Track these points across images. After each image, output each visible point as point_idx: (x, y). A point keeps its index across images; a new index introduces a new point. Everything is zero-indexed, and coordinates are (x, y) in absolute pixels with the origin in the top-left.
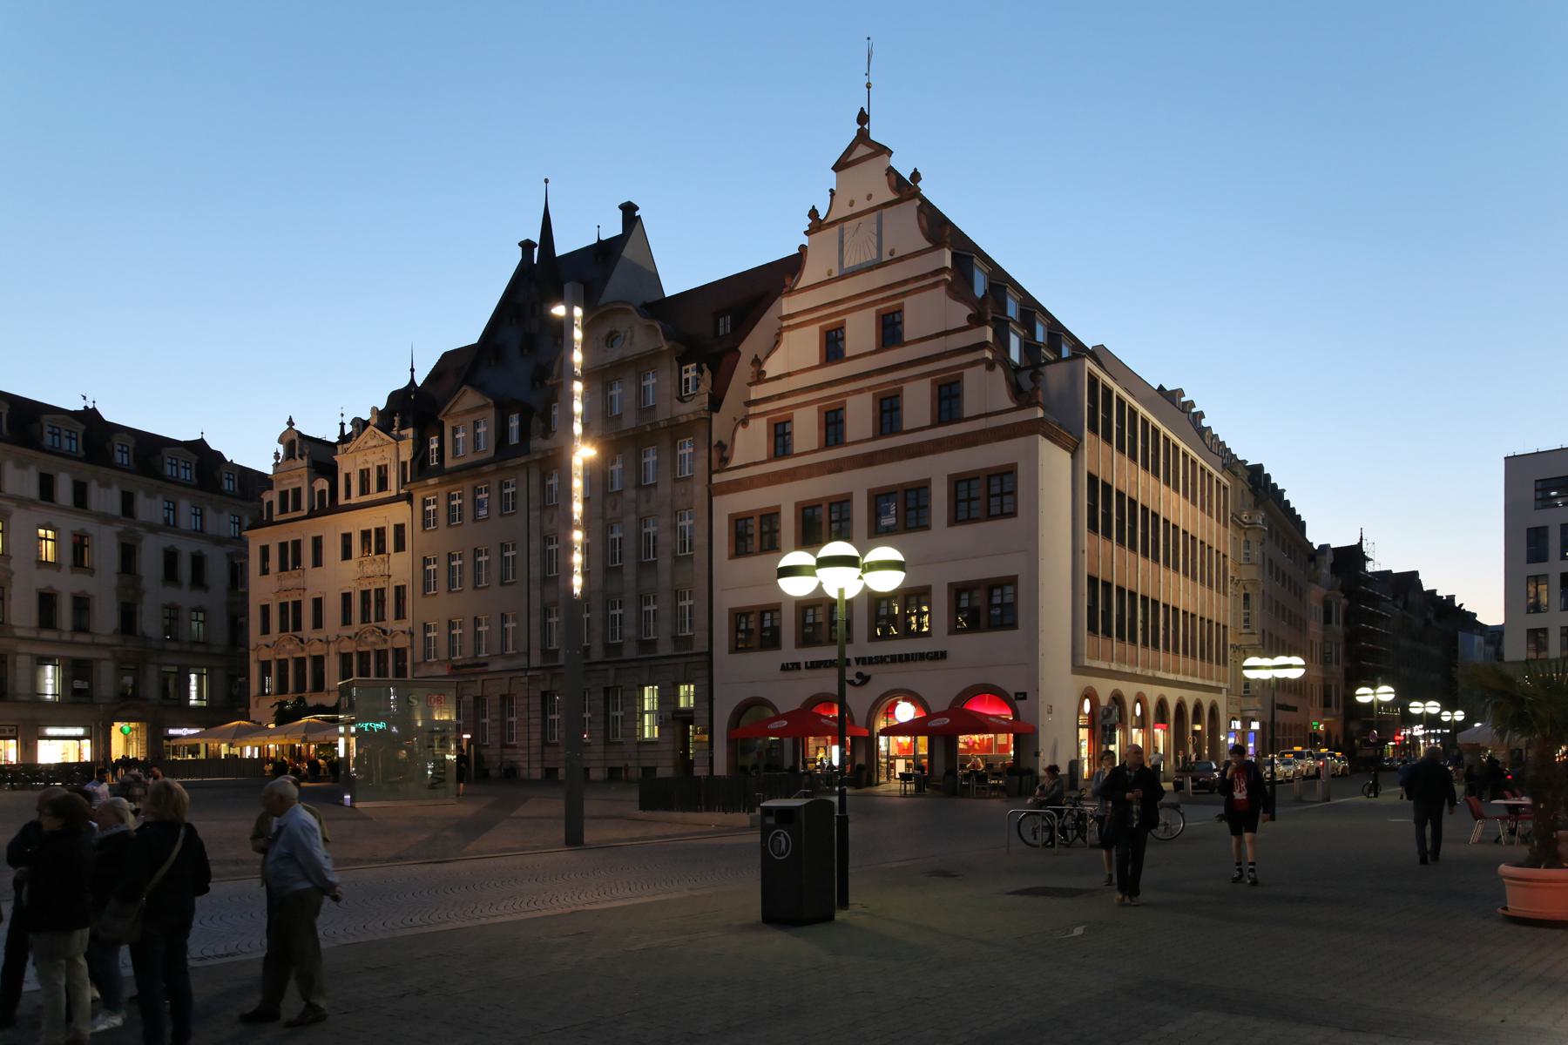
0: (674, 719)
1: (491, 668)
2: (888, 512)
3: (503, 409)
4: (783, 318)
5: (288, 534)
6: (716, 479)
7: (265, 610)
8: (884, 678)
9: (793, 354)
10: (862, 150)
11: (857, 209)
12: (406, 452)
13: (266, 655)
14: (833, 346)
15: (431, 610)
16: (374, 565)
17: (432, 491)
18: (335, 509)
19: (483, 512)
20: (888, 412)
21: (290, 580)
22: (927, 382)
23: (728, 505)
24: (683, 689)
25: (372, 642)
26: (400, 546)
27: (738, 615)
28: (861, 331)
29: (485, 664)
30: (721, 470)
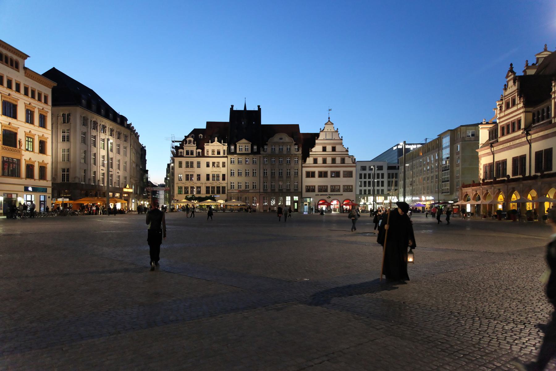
0: (293, 202)
5: (190, 160)
8: (332, 197)
9: (317, 149)
12: (225, 148)
13: (180, 185)
14: (324, 149)
15: (235, 180)
16: (215, 169)
17: (235, 157)
18: (203, 156)
20: (334, 161)
21: (189, 169)
23: (305, 170)
24: (297, 197)
26: (224, 166)
27: (307, 186)
28: (329, 148)
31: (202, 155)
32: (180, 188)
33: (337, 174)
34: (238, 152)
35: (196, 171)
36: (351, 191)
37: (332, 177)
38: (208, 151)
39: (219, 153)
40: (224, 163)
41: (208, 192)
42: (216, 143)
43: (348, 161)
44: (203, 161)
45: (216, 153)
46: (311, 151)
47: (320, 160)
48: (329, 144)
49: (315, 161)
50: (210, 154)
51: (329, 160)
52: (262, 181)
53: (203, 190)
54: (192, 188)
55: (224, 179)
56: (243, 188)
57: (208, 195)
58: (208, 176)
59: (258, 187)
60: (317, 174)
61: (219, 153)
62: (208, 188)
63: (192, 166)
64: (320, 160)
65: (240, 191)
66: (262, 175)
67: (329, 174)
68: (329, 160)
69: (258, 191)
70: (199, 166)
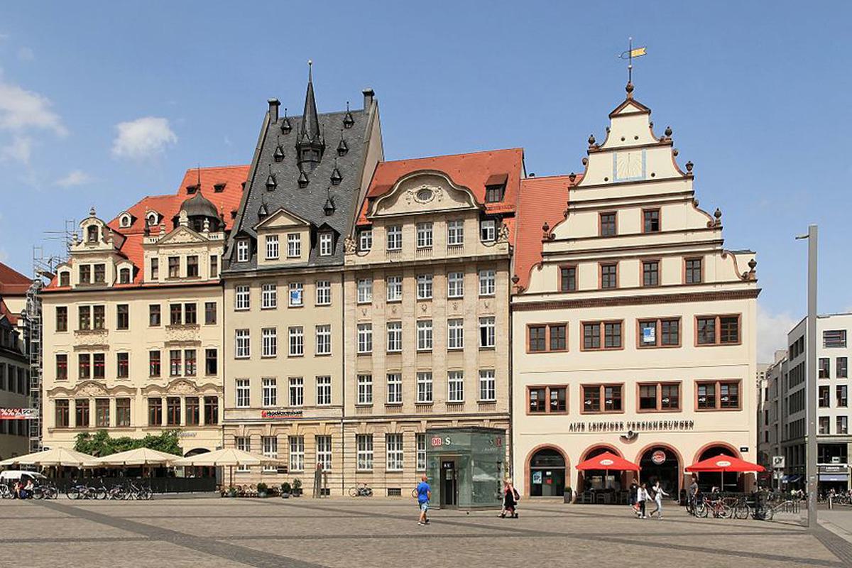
1: (304, 416)
2: (649, 333)
3: (315, 232)
4: (569, 203)
6: (515, 300)
7: (62, 360)
10: (630, 108)
11: (625, 144)
12: (218, 251)
16: (183, 334)
19: (297, 302)
22: (680, 259)
25: (182, 391)
26: (211, 319)
29: (301, 413)
30: (518, 295)
31: (131, 286)
32: (62, 405)
33: (669, 332)
34: (262, 260)
35: (114, 341)
36: (733, 403)
37: (643, 345)
38: (154, 268)
39: (193, 270)
40: (211, 308)
41: (155, 419)
42: (184, 236)
43: (717, 269)
44: (139, 309)
45: (183, 271)
46: (551, 239)
47: (589, 276)
48: (629, 202)
49: (568, 276)
50: (163, 275)
51: (630, 273)
52: (351, 373)
53: (139, 412)
54: (102, 403)
55: (212, 368)
56: (283, 400)
57: (157, 433)
58: (155, 356)
59: (336, 398)
60: (574, 336)
61: (193, 270)
62: (155, 403)
63: (100, 329)
64: (589, 276)
65: (268, 415)
66: (352, 347)
67: (630, 332)
68: (630, 273)
69: (338, 412)
70: (123, 322)
